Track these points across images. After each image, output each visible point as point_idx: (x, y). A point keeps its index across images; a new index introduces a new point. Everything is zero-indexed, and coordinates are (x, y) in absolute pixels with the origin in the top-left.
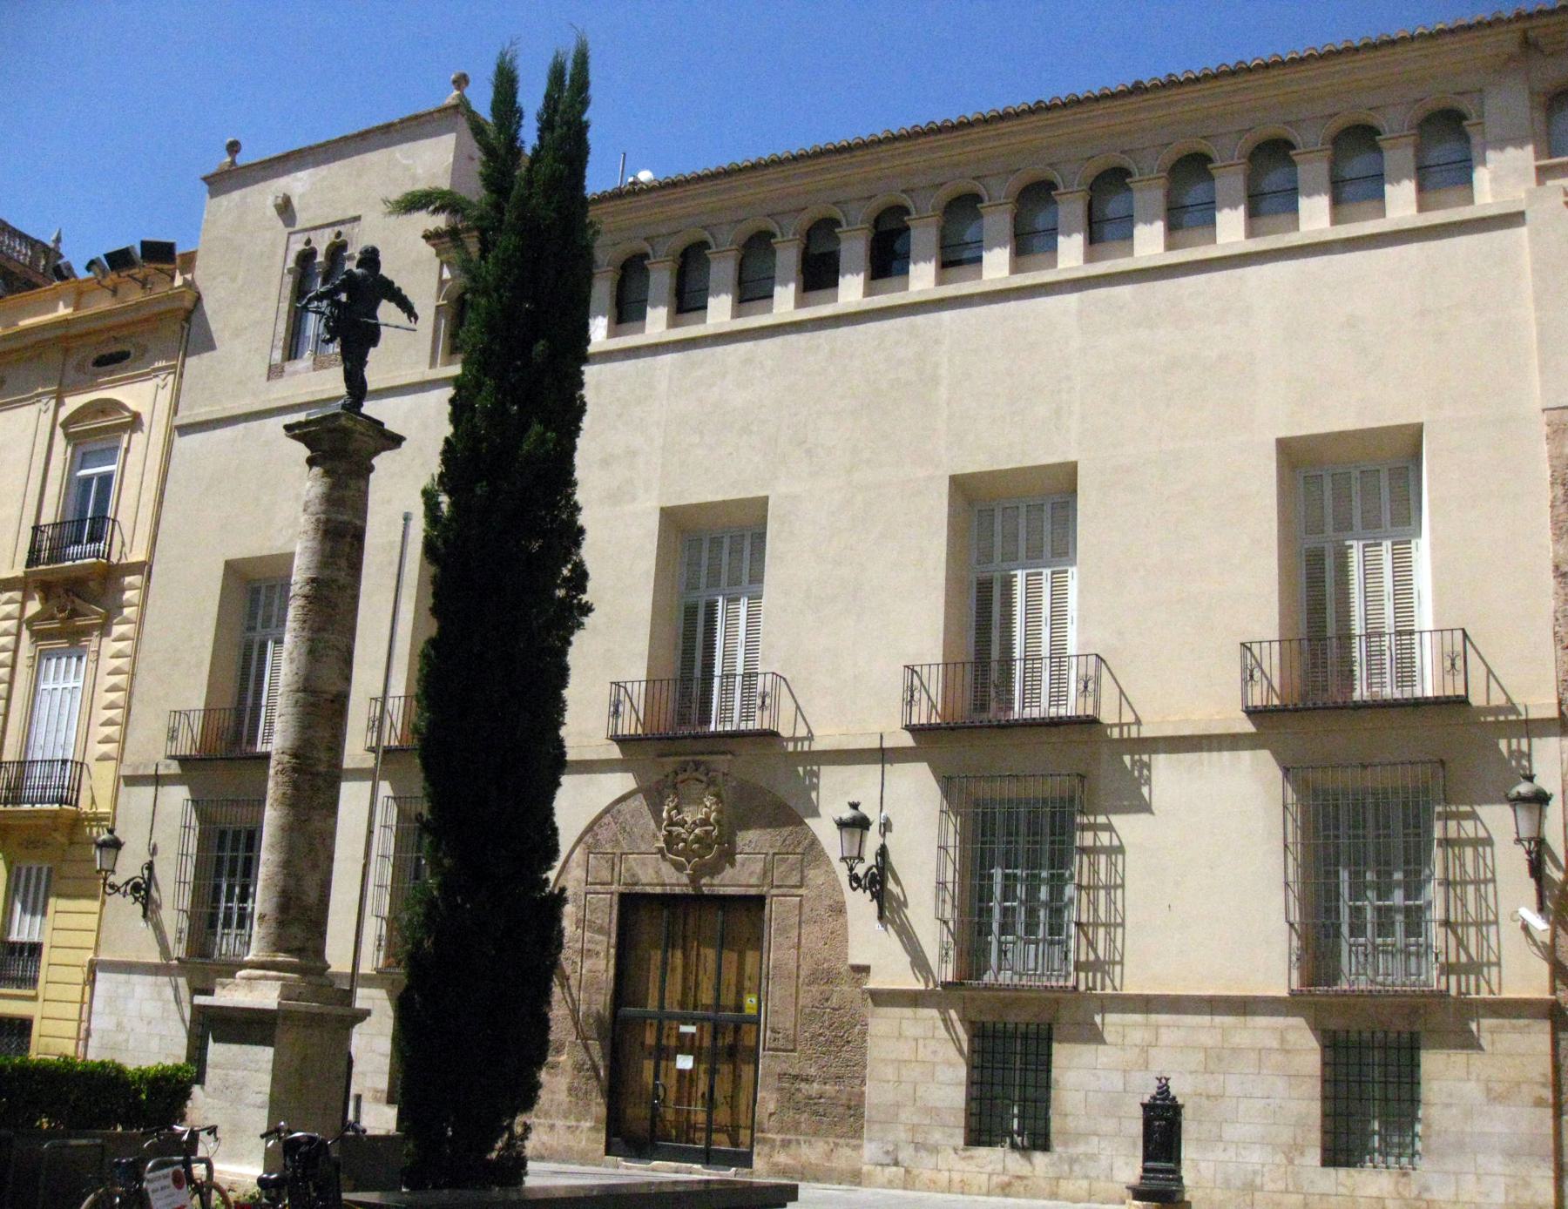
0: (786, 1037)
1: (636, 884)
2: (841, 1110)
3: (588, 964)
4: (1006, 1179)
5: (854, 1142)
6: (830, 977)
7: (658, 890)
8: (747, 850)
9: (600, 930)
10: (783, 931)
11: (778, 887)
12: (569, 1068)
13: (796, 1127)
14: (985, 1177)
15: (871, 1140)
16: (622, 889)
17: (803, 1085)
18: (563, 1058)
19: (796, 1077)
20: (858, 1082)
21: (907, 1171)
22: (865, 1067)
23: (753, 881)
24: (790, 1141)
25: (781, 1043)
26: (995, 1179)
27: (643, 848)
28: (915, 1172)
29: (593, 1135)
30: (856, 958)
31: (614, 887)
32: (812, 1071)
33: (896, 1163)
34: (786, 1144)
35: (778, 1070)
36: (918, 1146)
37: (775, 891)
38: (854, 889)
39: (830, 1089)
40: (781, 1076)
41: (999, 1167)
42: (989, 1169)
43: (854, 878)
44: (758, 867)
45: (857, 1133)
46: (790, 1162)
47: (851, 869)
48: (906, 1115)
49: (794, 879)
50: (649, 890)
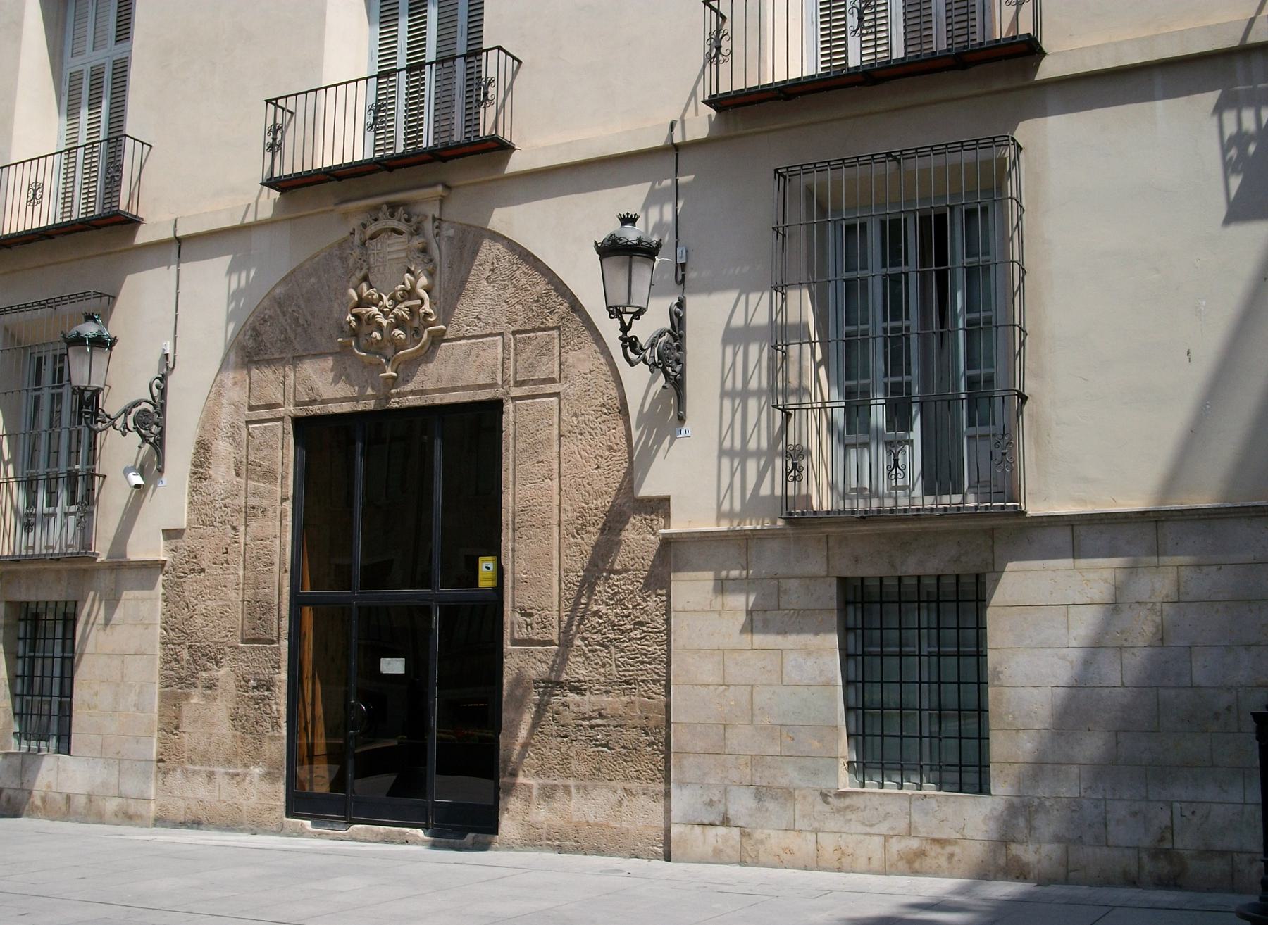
1: (313, 402)
3: (254, 525)
4: (914, 844)
7: (347, 407)
9: (269, 476)
11: (523, 383)
12: (232, 686)
13: (564, 766)
14: (878, 841)
17: (572, 697)
18: (222, 673)
21: (745, 834)
23: (483, 379)
24: (554, 788)
26: (896, 846)
28: (758, 834)
29: (266, 787)
31: (280, 412)
33: (726, 822)
34: (548, 793)
36: (761, 791)
38: (632, 364)
39: (614, 702)
41: (902, 825)
42: (883, 828)
43: (630, 344)
46: (557, 821)
47: (625, 328)
48: (740, 738)
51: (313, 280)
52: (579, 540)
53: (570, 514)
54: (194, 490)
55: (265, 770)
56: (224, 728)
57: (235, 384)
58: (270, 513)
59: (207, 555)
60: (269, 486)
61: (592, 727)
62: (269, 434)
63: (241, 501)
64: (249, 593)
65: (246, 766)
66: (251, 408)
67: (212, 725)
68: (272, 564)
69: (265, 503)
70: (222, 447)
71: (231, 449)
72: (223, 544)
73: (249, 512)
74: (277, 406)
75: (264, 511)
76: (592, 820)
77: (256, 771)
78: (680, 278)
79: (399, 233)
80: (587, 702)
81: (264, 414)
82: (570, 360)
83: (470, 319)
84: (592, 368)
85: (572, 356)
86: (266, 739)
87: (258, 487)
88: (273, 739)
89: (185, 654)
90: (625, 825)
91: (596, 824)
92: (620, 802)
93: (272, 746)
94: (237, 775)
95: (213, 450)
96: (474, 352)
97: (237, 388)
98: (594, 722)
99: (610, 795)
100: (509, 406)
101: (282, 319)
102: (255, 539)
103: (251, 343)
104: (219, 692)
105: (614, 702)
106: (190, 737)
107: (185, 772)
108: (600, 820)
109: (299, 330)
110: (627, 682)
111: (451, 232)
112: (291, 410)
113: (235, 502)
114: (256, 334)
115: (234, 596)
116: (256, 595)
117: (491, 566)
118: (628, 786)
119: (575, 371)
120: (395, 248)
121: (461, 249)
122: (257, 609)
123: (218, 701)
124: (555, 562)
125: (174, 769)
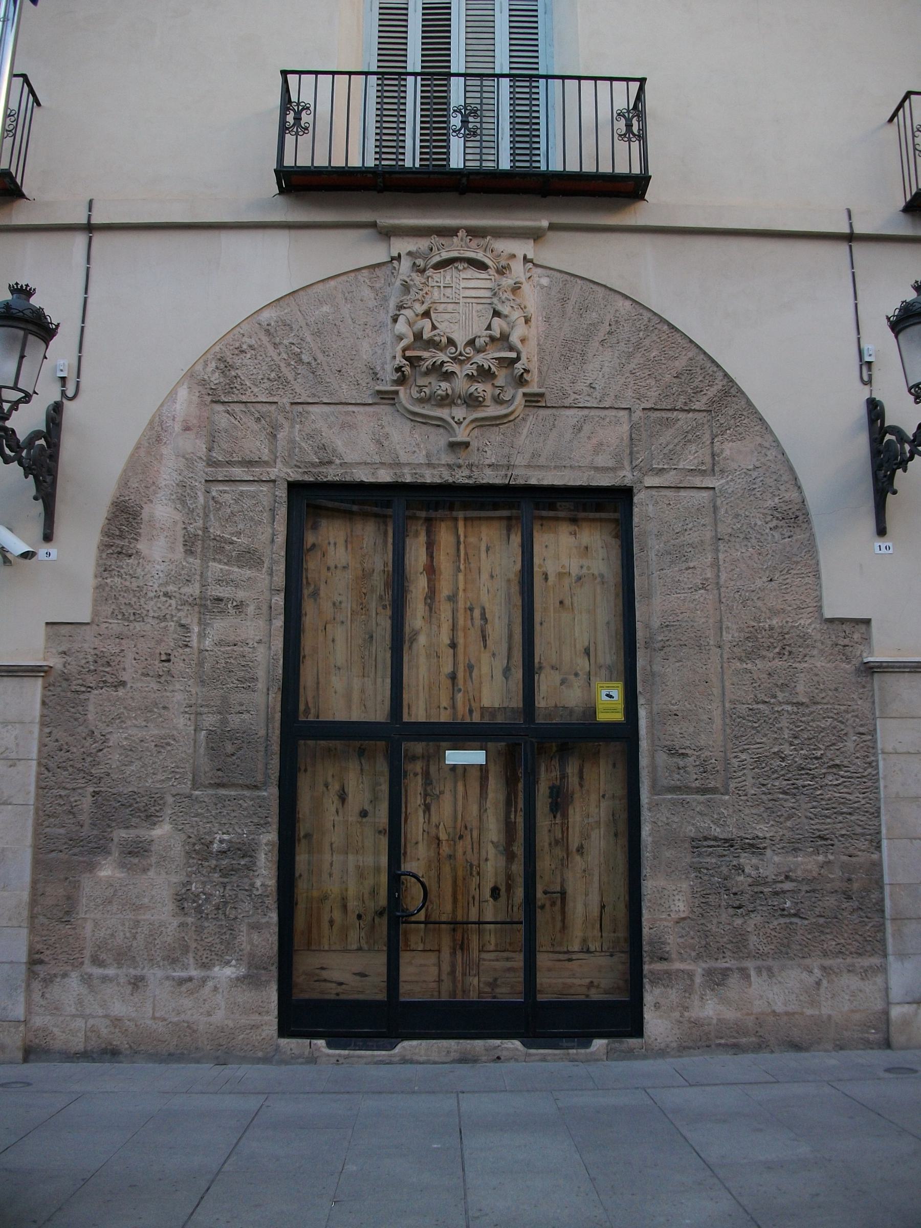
0: (704, 767)
2: (831, 901)
3: (219, 627)
5: (866, 962)
6: (786, 645)
7: (384, 476)
8: (583, 401)
9: (249, 558)
10: (678, 555)
12: (177, 850)
13: (739, 943)
15: (902, 956)
16: (295, 476)
17: (747, 860)
18: (162, 831)
19: (729, 842)
20: (862, 844)
22: (877, 814)
23: (602, 460)
24: (725, 973)
25: (693, 778)
27: (346, 392)
29: (246, 996)
30: (837, 605)
31: (274, 472)
32: (763, 829)
34: (717, 979)
35: (690, 831)
37: (649, 481)
39: (806, 863)
40: (698, 843)
44: (615, 432)
45: (874, 944)
46: (730, 1014)
49: (692, 457)
50: (363, 475)
51: (326, 309)
52: (749, 666)
53: (736, 635)
54: (104, 570)
55: (243, 971)
56: (163, 914)
57: (187, 429)
58: (251, 609)
59: (129, 661)
60: (248, 573)
61: (776, 893)
62: (248, 503)
63: (194, 589)
64: (210, 720)
65: (205, 966)
66: (212, 463)
67: (138, 908)
68: (254, 679)
69: (241, 595)
70: (162, 511)
71: (178, 517)
72: (163, 648)
73: (210, 606)
74: (266, 463)
75: (240, 607)
76: (779, 1008)
77: (226, 973)
78: (866, 378)
79: (481, 266)
80: (771, 864)
81: (238, 472)
82: (727, 453)
83: (580, 386)
84: (758, 464)
85: (728, 449)
86: (244, 928)
87: (229, 573)
88: (256, 927)
89: (86, 803)
90: (825, 1011)
91: (787, 1013)
92: (818, 983)
93: (255, 936)
94: (190, 979)
95: (145, 515)
96: (587, 428)
97: (191, 435)
98: (779, 887)
99: (805, 975)
100: (639, 498)
101: (270, 348)
102: (220, 643)
103: (216, 378)
104: (153, 860)
105: (806, 863)
106: (95, 923)
107: (87, 980)
108: (790, 1008)
109: (301, 369)
110: (821, 838)
111: (545, 281)
112: (285, 472)
113: (183, 591)
114: (225, 366)
115: (182, 723)
116: (224, 722)
117: (614, 693)
118: (828, 962)
119: (735, 466)
120: (472, 284)
121: (564, 301)
122: (222, 744)
123: (151, 873)
124: (716, 691)
125: (65, 975)
